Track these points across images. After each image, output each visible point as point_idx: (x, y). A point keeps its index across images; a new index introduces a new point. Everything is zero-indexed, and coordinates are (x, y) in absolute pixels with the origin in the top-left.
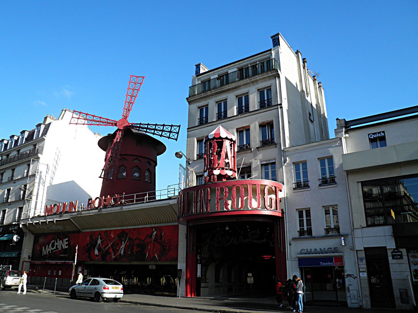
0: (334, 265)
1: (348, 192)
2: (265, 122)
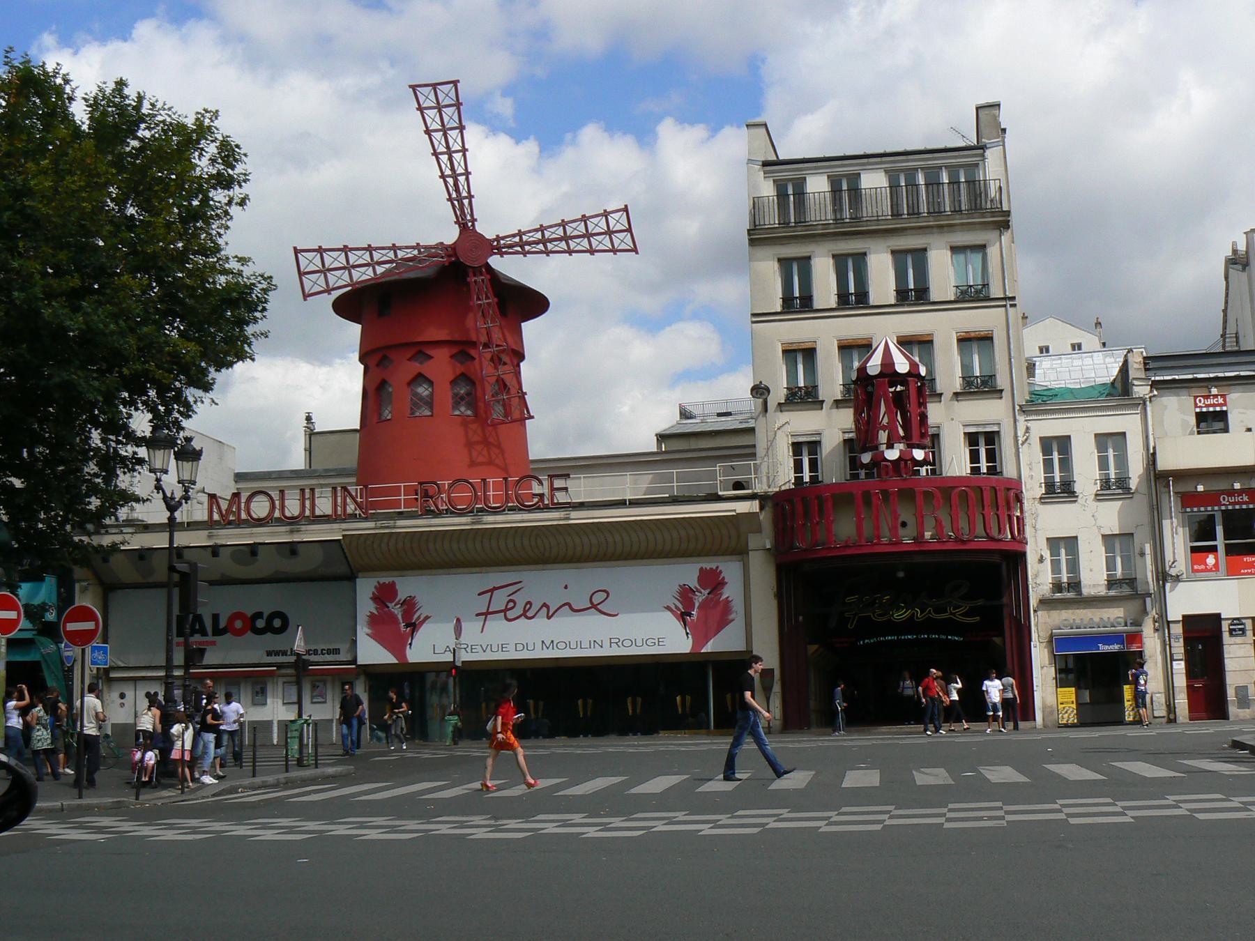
0: (1126, 650)
1: (1156, 512)
2: (973, 335)
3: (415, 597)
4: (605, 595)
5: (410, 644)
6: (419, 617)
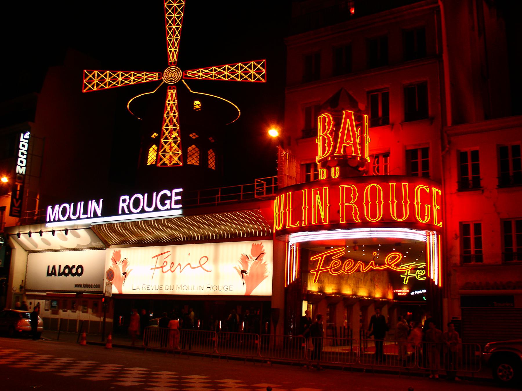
3: (127, 259)
4: (206, 259)
5: (124, 284)
6: (128, 270)
